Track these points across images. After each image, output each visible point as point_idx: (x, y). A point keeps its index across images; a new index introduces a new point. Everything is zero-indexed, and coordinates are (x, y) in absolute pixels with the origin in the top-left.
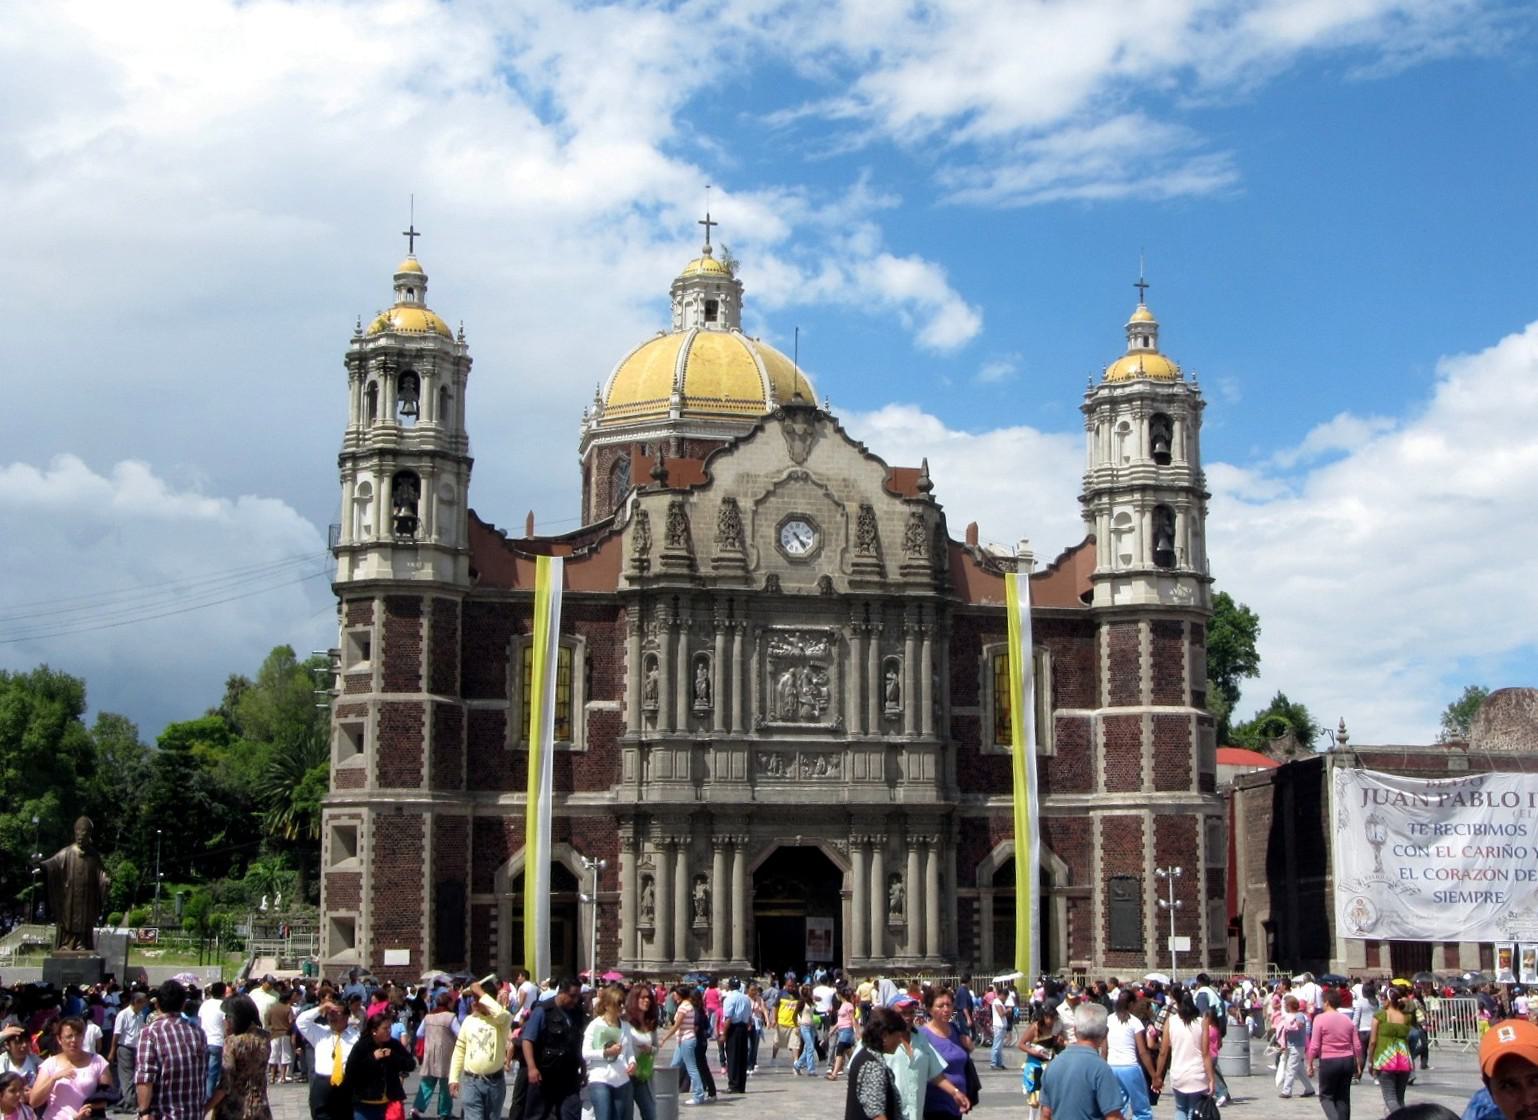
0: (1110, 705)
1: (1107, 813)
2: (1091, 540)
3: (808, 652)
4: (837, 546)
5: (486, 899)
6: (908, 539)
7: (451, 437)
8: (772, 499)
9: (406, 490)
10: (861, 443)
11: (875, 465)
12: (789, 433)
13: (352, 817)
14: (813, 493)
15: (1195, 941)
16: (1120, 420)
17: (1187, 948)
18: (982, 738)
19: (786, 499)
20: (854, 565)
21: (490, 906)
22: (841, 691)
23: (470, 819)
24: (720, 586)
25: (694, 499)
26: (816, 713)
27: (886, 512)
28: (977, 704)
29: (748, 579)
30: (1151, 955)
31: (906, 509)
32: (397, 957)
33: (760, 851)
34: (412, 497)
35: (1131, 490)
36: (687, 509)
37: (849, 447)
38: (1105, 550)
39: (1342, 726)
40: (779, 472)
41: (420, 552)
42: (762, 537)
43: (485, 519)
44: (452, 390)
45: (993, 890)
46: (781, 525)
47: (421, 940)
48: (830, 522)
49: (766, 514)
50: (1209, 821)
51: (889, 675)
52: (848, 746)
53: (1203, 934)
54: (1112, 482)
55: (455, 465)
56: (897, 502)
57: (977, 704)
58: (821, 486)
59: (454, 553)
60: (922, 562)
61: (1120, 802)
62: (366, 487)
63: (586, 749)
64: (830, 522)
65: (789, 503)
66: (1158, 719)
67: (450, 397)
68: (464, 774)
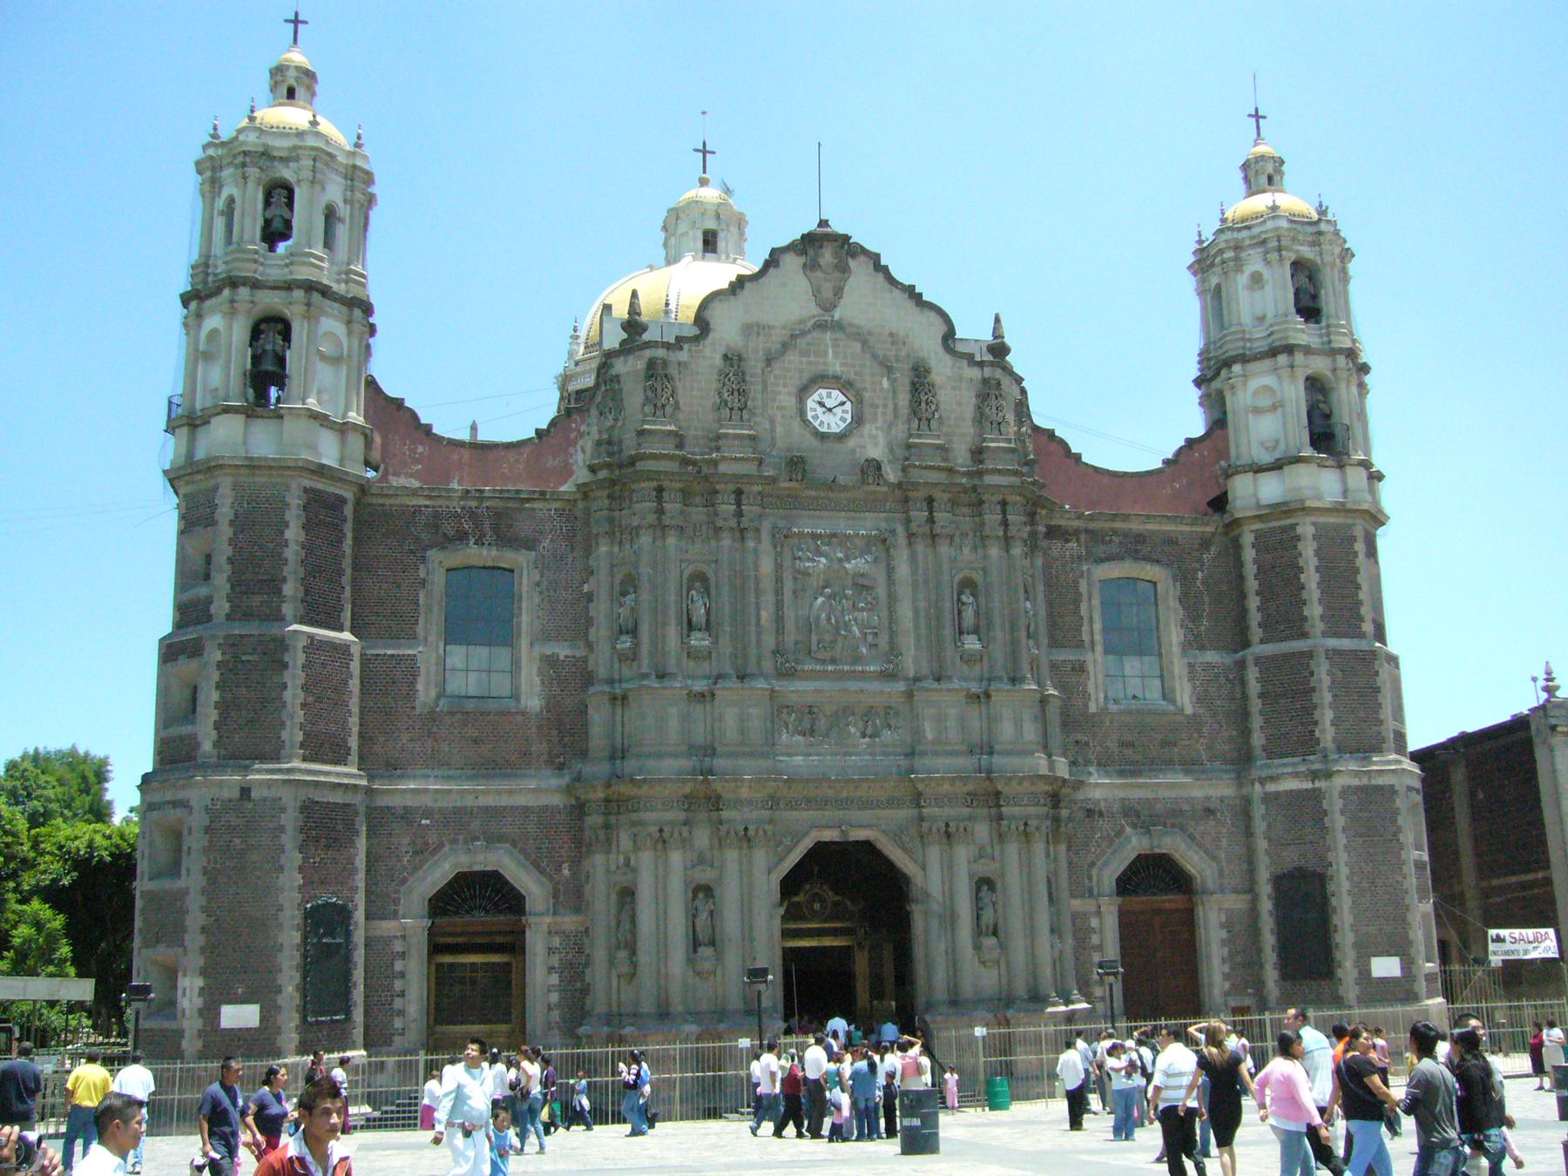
0: (1262, 642)
1: (1271, 787)
2: (1218, 423)
5: (387, 927)
6: (982, 414)
9: (271, 341)
10: (913, 287)
11: (932, 315)
12: (811, 267)
13: (175, 804)
14: (849, 351)
15: (1407, 965)
16: (1249, 270)
18: (1091, 689)
21: (396, 937)
22: (892, 620)
23: (362, 809)
24: (724, 468)
25: (683, 356)
26: (864, 650)
28: (1080, 645)
30: (1350, 990)
31: (975, 373)
32: (240, 1016)
33: (790, 850)
34: (278, 349)
35: (1273, 353)
36: (673, 371)
37: (897, 293)
39: (1548, 673)
40: (801, 322)
41: (287, 419)
43: (391, 390)
44: (343, 210)
45: (1119, 900)
46: (803, 391)
47: (279, 990)
48: (874, 390)
53: (1419, 949)
54: (1244, 348)
55: (344, 309)
56: (965, 363)
57: (1080, 645)
59: (344, 429)
61: (1289, 770)
62: (214, 333)
63: (538, 708)
66: (1334, 655)
67: (341, 220)
68: (354, 743)
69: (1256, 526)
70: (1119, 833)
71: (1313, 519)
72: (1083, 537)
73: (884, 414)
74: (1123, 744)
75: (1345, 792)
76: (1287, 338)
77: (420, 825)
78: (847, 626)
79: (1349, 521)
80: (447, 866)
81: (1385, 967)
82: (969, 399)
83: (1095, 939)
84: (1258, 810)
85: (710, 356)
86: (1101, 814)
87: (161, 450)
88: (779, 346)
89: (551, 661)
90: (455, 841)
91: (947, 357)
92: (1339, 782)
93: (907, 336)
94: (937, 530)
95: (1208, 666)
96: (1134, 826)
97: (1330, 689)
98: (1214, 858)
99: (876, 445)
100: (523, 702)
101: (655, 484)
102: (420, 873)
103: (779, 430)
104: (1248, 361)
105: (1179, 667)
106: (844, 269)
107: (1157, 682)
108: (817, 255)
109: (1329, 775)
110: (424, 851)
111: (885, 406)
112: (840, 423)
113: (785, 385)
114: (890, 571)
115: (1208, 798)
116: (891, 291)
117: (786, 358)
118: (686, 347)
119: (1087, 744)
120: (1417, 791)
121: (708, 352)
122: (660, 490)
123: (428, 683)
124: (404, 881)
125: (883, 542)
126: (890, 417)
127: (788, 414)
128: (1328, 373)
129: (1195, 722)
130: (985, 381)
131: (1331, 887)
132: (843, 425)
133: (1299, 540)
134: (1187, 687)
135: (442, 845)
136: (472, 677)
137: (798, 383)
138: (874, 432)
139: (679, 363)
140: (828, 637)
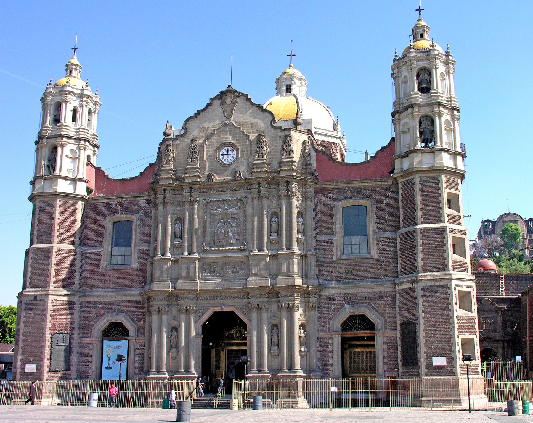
0: (403, 228)
1: (401, 287)
4: (247, 156)
5: (87, 340)
7: (77, 129)
11: (267, 114)
12: (222, 104)
14: (235, 132)
17: (445, 364)
18: (334, 250)
21: (90, 344)
28: (333, 234)
30: (423, 370)
33: (203, 314)
35: (407, 108)
37: (254, 108)
38: (398, 143)
44: (80, 110)
46: (219, 149)
49: (211, 145)
50: (458, 289)
51: (273, 220)
57: (333, 234)
61: (405, 280)
65: (223, 138)
69: (403, 180)
70: (342, 307)
71: (420, 175)
72: (335, 191)
73: (247, 154)
74: (347, 272)
75: (424, 288)
76: (411, 102)
77: (99, 307)
78: (228, 233)
79: (437, 174)
80: (105, 321)
81: (439, 361)
83: (330, 348)
84: (397, 296)
85: (187, 140)
86: (335, 299)
87: (28, 191)
89: (141, 251)
90: (108, 312)
91: (272, 129)
92: (421, 284)
94: (261, 195)
95: (385, 239)
96: (348, 304)
97: (422, 246)
98: (382, 316)
100: (132, 265)
101: (163, 188)
102: (98, 323)
104: (401, 113)
105: (372, 239)
106: (234, 103)
107: (366, 246)
108: (225, 99)
109: (417, 281)
110: (100, 316)
112: (232, 159)
113: (212, 148)
114: (245, 211)
115: (381, 292)
116: (252, 107)
118: (179, 138)
119: (332, 272)
120: (468, 287)
121: (186, 140)
122: (165, 190)
123: (104, 260)
124: (93, 325)
125: (241, 201)
126: (248, 155)
127: (212, 158)
128: (431, 114)
129: (378, 261)
130: (286, 137)
131: (417, 328)
132: (233, 159)
133: (414, 185)
134: (376, 247)
135: (104, 314)
136: (119, 257)
138: (243, 161)
139: (176, 144)
140: (221, 238)
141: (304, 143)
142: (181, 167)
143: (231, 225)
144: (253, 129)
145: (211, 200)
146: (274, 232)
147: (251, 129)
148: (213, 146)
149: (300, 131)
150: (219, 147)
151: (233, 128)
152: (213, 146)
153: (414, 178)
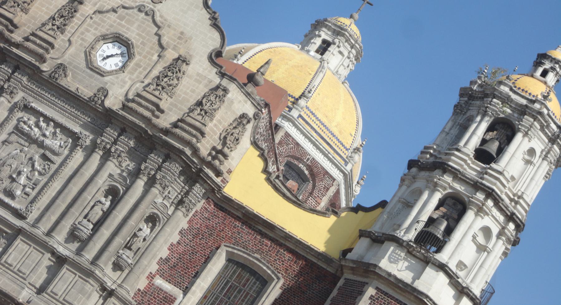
3: (48, 142)
4: (138, 77)
6: (199, 104)
8: (112, 16)
11: (216, 35)
14: (148, 29)
19: (123, 23)
20: (138, 95)
26: (18, 192)
27: (198, 74)
29: (42, 59)
31: (217, 80)
37: (204, 11)
42: (83, 39)
46: (104, 38)
48: (145, 57)
52: (19, 231)
58: (159, 27)
60: (198, 124)
64: (145, 57)
65: (123, 26)
73: (140, 73)
78: (19, 173)
82: (201, 90)
88: (110, 7)
93: (191, 38)
99: (122, 87)
103: (72, 50)
111: (145, 69)
113: (96, 29)
116: (202, 10)
117: (108, 15)
126: (142, 76)
132: (114, 68)
137: (104, 31)
141: (243, 116)
142: (28, 27)
143: (33, 166)
144: (178, 43)
145: (33, 105)
146: (89, 221)
147: (175, 41)
148: (99, 28)
149: (248, 95)
150: (107, 35)
151: (149, 21)
152: (99, 28)
153: (367, 283)
